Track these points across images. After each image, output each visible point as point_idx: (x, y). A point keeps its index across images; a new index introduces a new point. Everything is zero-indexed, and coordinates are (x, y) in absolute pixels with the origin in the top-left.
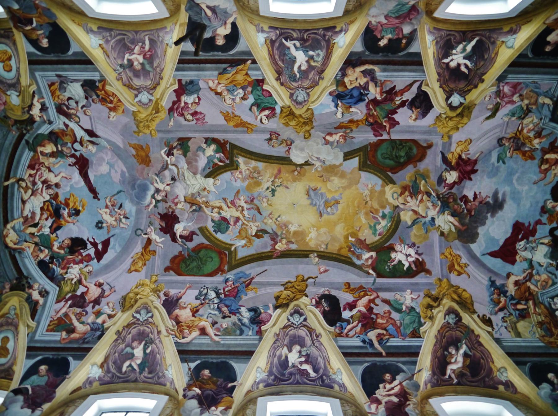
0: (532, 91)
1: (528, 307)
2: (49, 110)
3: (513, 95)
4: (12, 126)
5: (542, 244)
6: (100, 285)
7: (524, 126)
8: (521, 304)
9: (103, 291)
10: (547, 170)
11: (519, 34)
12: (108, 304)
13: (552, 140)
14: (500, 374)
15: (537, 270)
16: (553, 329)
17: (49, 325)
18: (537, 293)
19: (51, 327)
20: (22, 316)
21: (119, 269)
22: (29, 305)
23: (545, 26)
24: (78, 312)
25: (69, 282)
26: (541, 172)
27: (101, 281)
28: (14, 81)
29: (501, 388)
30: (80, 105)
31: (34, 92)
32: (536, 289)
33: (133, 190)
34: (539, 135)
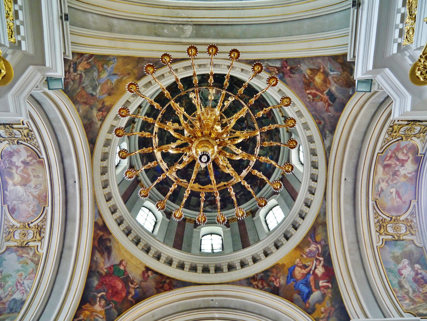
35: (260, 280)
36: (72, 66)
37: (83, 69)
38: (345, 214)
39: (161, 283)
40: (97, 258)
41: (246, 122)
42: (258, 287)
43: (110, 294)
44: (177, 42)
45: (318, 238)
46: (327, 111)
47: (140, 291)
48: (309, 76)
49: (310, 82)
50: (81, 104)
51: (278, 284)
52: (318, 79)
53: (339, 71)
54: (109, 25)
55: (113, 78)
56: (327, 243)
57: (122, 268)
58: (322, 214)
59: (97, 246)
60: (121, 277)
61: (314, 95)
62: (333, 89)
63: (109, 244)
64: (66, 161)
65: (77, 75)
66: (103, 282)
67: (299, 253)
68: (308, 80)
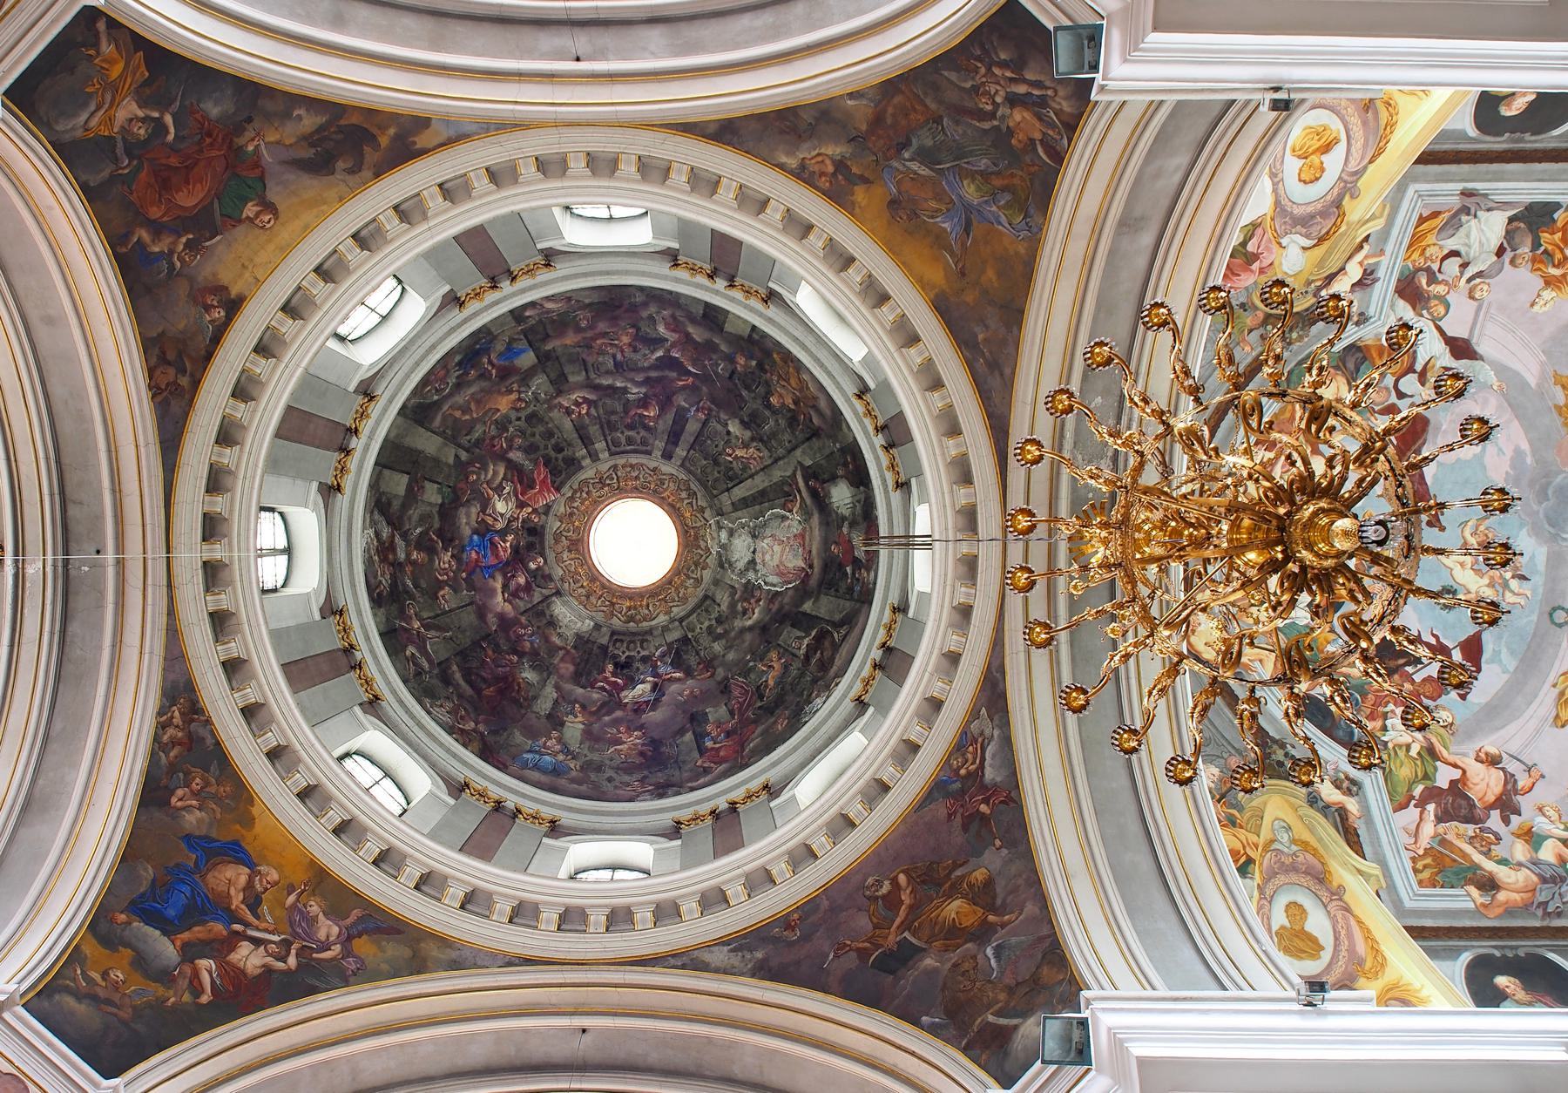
2: (1378, 285)
4: (1250, 331)
6: (1493, 761)
9: (1510, 778)
12: (1540, 809)
17: (1415, 871)
19: (1426, 875)
20: (1325, 847)
21: (1526, 715)
22: (1326, 817)
24: (1471, 833)
25: (1402, 753)
27: (1493, 750)
28: (1310, 209)
30: (1468, 274)
31: (1366, 239)
33: (1540, 503)
35: (190, 735)
36: (1036, 92)
37: (1011, 124)
38: (458, 1039)
39: (180, 355)
40: (300, 118)
41: (678, 675)
42: (162, 726)
43: (163, 161)
44: (1062, 436)
45: (363, 946)
46: (840, 948)
47: (159, 273)
48: (963, 877)
49: (940, 885)
50: (876, 107)
51: (179, 804)
52: (954, 908)
53: (1002, 973)
54: (1142, 218)
55: (956, 220)
56: (352, 979)
57: (250, 210)
58: (454, 954)
59: (343, 122)
60: (216, 205)
61: (892, 901)
62: (929, 962)
63: (340, 165)
64: (655, 35)
65: (994, 102)
66: (209, 135)
67: (299, 877)
68: (948, 876)
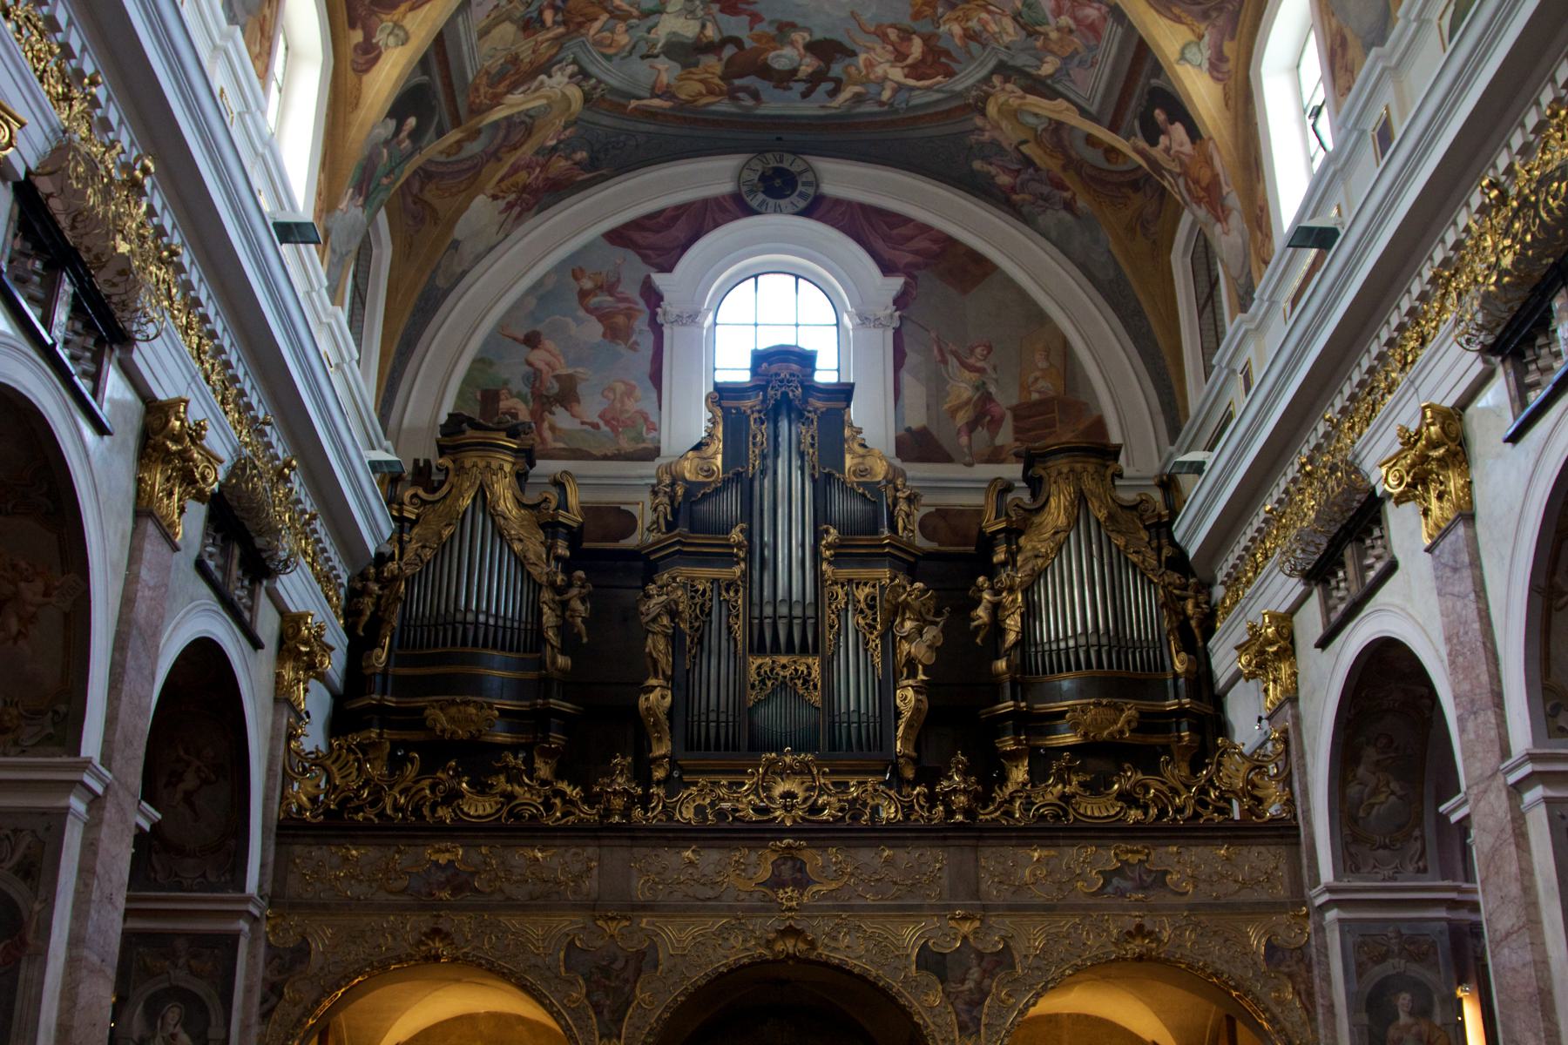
0: (1076, 52)
1: (548, 29)
3: (1075, 18)
5: (703, 26)
7: (997, 17)
8: (556, 14)
10: (884, 37)
11: (1206, 76)
13: (954, 54)
14: (388, 31)
15: (638, 26)
16: (507, 82)
18: (582, 35)
23: (1205, 137)
26: (879, 26)
29: (357, 36)
32: (592, 32)
34: (970, 35)
